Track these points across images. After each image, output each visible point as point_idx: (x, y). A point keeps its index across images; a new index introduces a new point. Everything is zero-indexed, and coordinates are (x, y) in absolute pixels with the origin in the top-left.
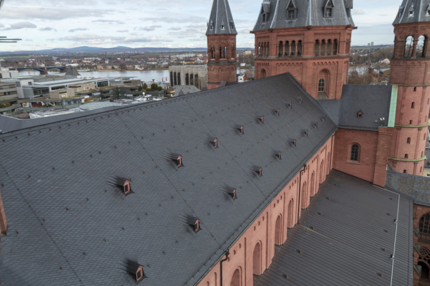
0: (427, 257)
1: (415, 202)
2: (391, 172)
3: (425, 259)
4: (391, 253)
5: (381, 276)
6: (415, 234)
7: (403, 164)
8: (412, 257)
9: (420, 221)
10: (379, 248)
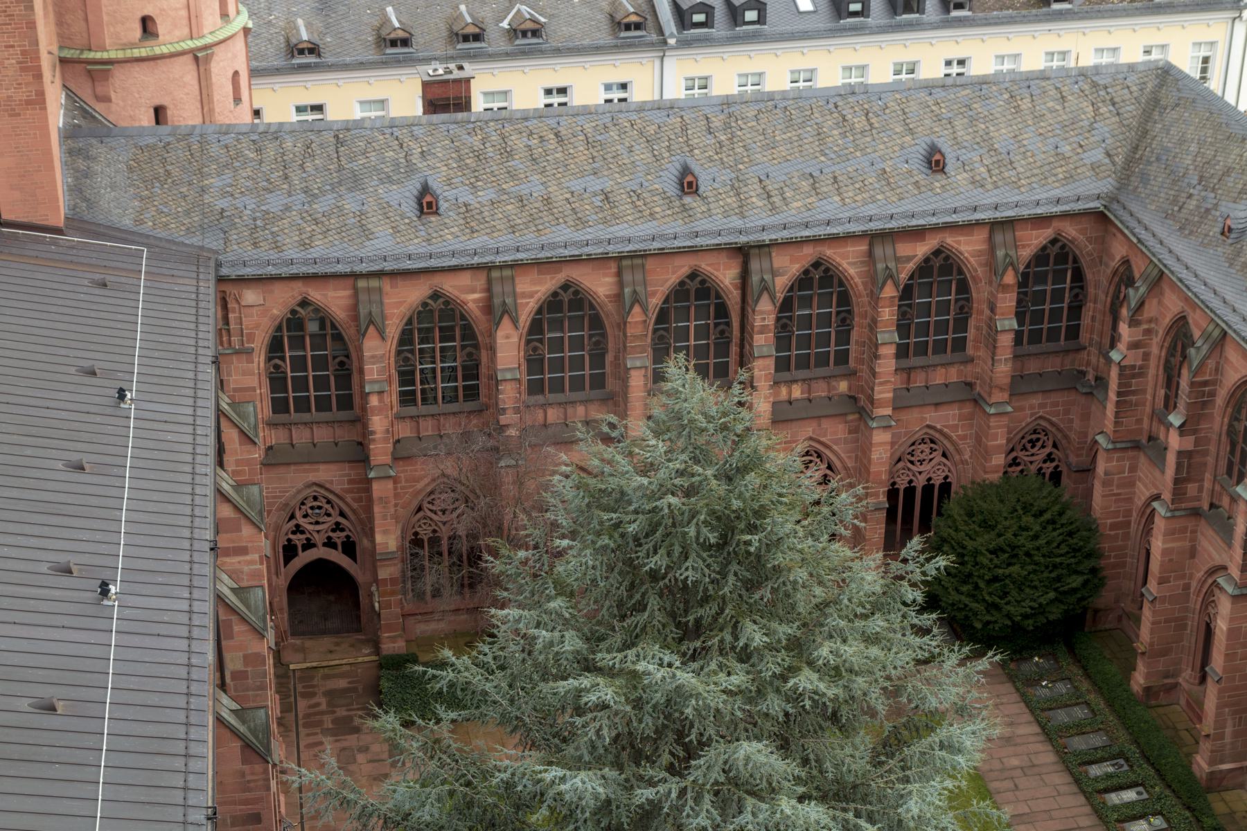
0: (338, 527)
1: (225, 271)
2: (87, 128)
3: (330, 544)
4: (106, 575)
5: (52, 709)
6: (242, 432)
7: (139, 74)
8: (208, 558)
9: (269, 359)
10: (44, 568)
